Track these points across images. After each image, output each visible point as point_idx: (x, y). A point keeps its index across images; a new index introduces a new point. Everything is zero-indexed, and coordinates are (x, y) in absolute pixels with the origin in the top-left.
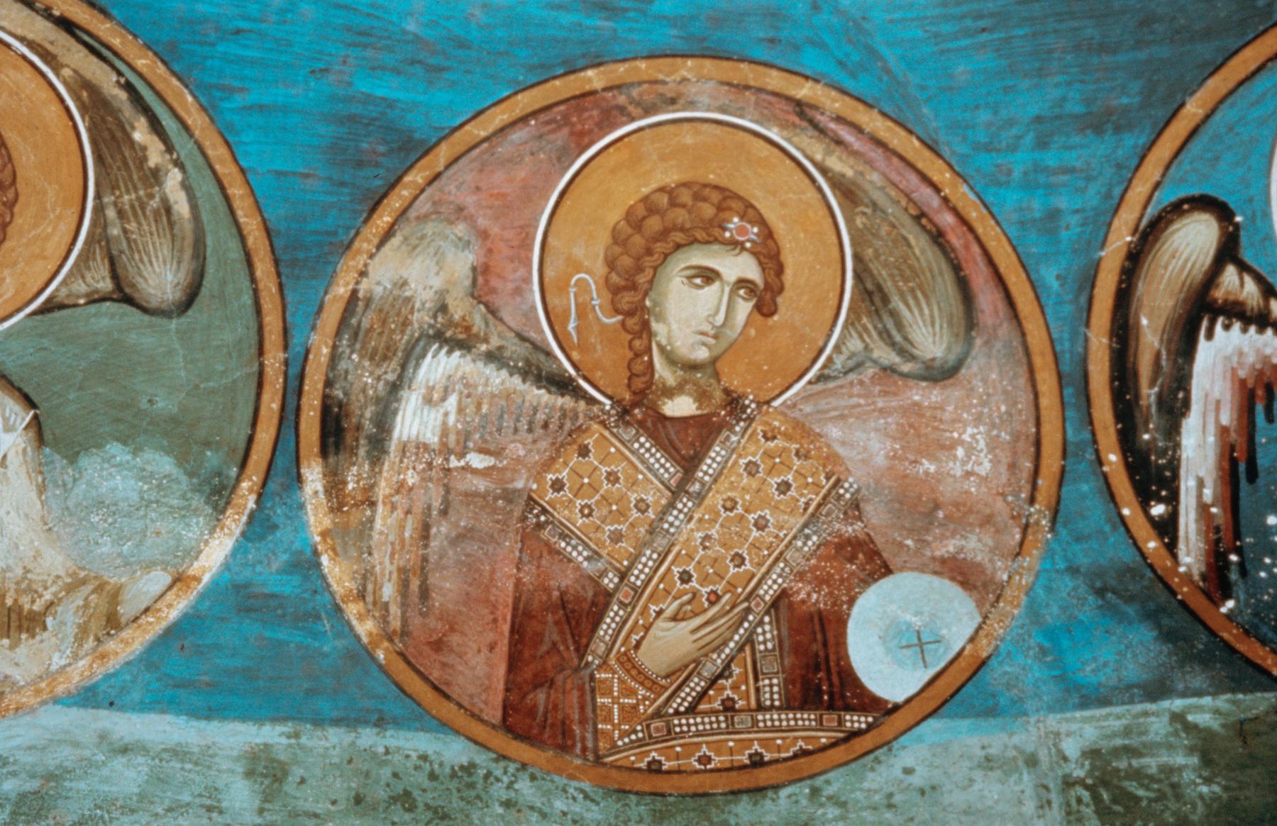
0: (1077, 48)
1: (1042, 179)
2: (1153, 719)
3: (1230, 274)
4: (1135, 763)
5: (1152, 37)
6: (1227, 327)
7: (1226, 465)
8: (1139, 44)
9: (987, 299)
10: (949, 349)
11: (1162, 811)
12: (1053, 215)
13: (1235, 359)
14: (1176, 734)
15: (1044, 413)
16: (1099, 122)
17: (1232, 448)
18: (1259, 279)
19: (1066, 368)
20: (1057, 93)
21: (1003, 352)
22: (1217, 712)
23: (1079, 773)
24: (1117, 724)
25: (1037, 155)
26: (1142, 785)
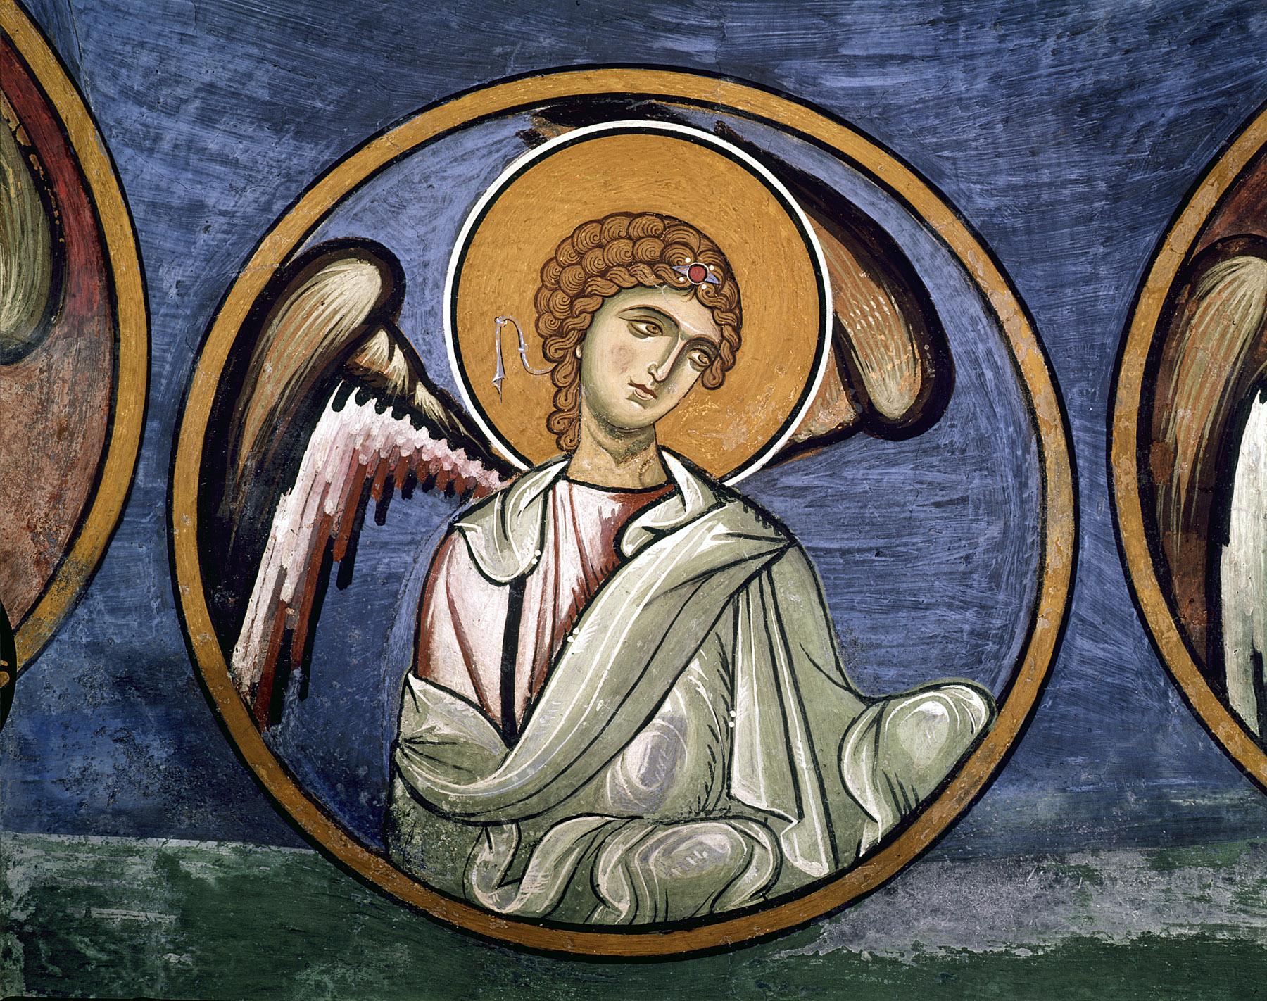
0: (282, 22)
1: (194, 160)
2: (137, 859)
3: (381, 341)
4: (95, 912)
5: (367, 43)
6: (361, 401)
7: (318, 561)
8: (351, 47)
9: (83, 282)
10: (17, 327)
11: (112, 980)
12: (196, 208)
13: (360, 440)
14: (156, 883)
15: (115, 442)
16: (280, 118)
17: (331, 542)
18: (411, 356)
19: (157, 396)
20: (244, 66)
21: (84, 353)
22: (218, 862)
23: (21, 916)
24: (85, 860)
25: (199, 131)
26: (94, 942)
